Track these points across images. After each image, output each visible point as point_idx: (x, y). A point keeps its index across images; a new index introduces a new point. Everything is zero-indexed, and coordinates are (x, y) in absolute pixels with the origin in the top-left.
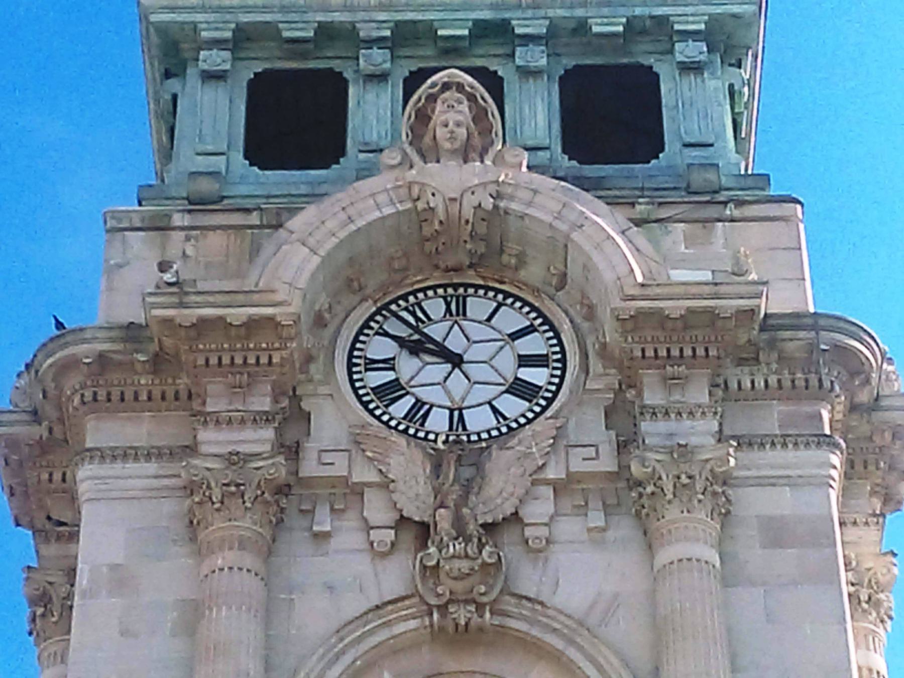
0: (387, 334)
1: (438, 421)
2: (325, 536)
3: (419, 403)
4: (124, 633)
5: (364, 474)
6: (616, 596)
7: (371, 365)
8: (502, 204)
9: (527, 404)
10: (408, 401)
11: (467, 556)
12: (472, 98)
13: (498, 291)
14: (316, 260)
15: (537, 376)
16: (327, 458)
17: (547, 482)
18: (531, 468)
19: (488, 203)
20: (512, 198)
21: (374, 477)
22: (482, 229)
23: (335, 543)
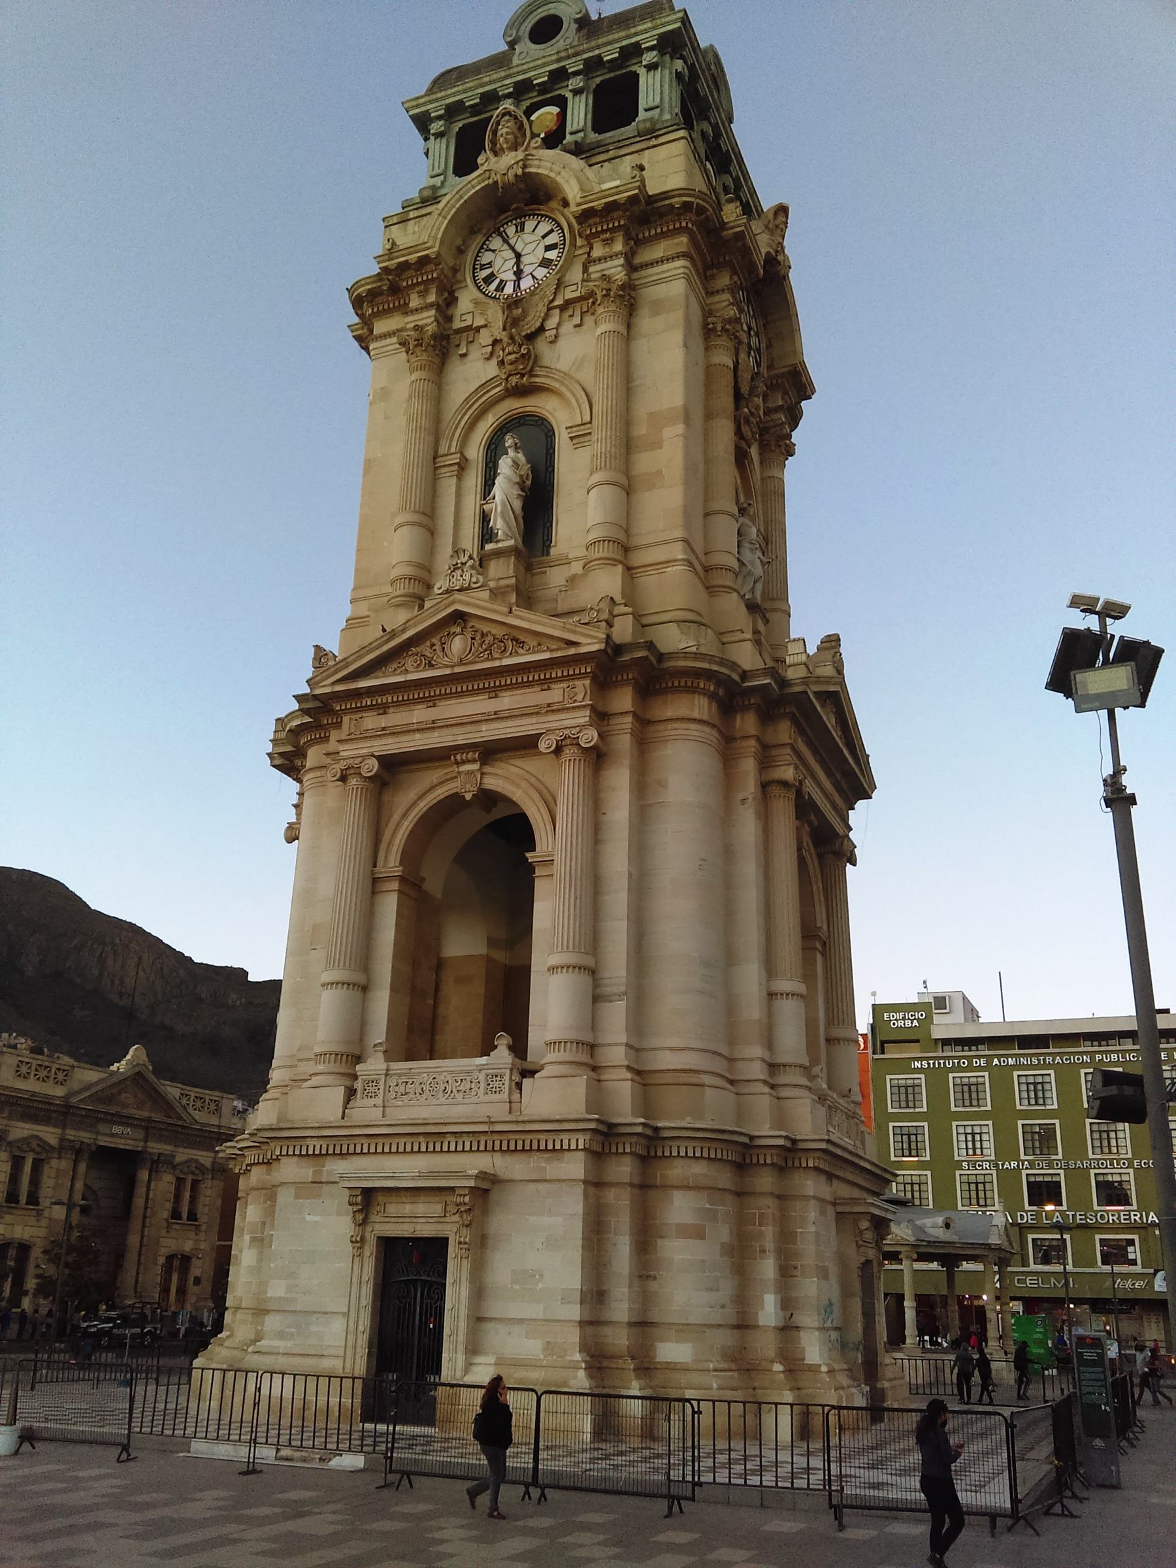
0: (490, 250)
1: (509, 289)
2: (464, 356)
3: (501, 281)
4: (386, 418)
5: (479, 322)
6: (584, 356)
7: (483, 267)
8: (527, 170)
9: (547, 270)
10: (497, 281)
11: (514, 353)
12: (516, 118)
13: (538, 215)
14: (446, 222)
15: (552, 255)
16: (464, 318)
17: (556, 307)
18: (546, 301)
19: (520, 172)
20: (531, 166)
21: (482, 322)
22: (522, 186)
23: (470, 357)
